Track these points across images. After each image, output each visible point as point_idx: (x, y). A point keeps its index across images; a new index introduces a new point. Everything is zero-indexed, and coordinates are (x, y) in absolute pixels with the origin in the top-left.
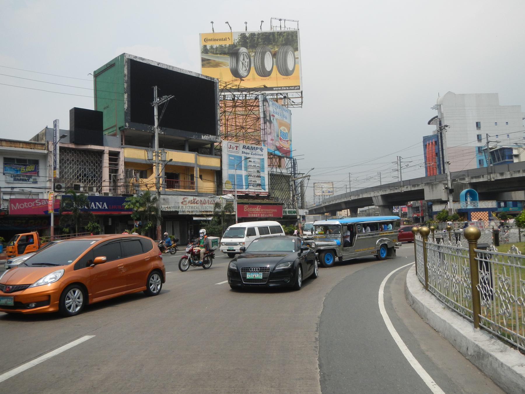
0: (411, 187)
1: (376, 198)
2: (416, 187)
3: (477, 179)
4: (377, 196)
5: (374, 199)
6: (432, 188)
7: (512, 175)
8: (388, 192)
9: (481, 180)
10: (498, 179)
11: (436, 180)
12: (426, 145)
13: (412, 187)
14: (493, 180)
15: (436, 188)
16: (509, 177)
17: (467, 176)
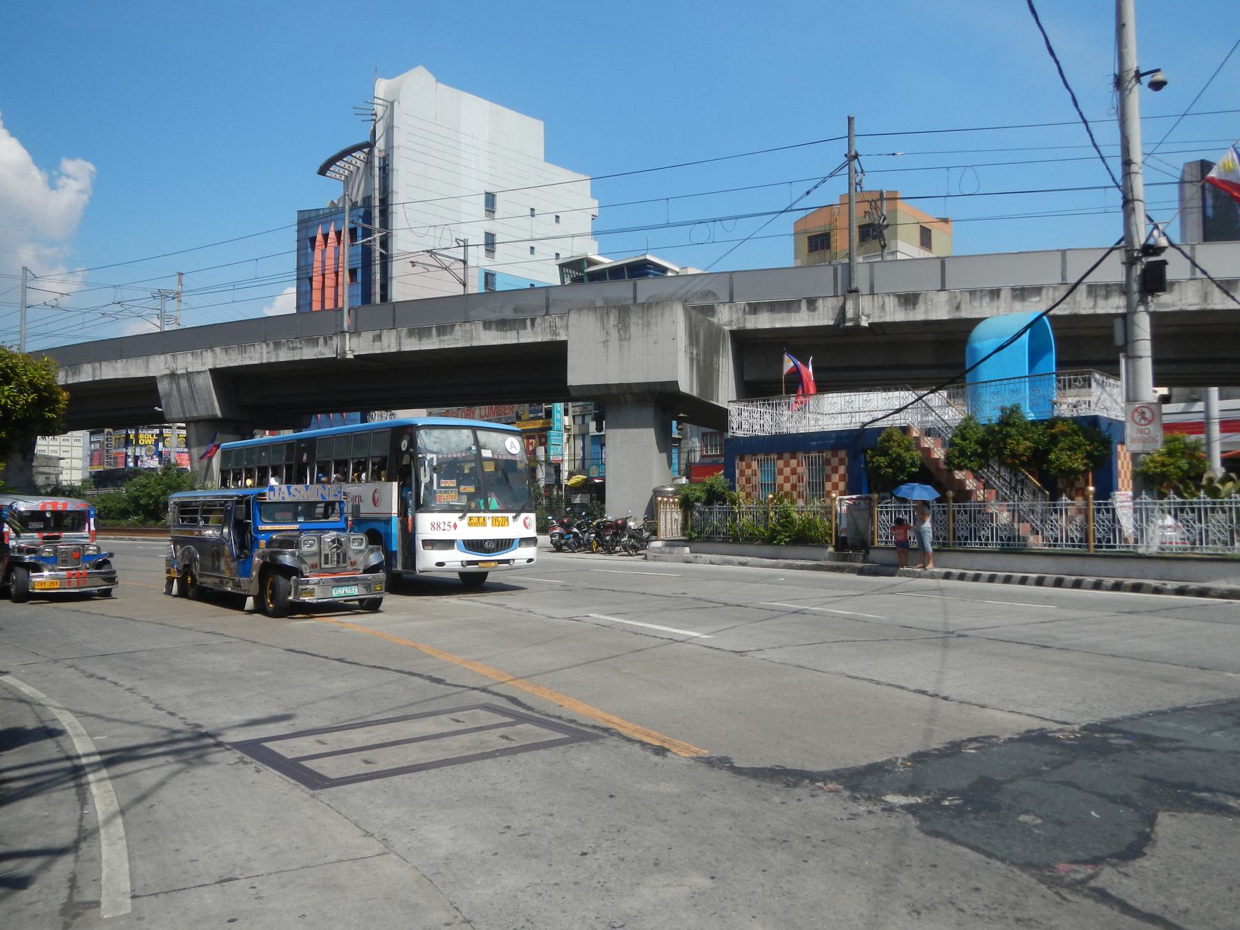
0: (399, 338)
1: (184, 383)
2: (429, 335)
3: (778, 316)
4: (189, 375)
5: (163, 387)
6: (623, 326)
7: (958, 308)
8: (258, 355)
9: (801, 319)
10: (889, 319)
11: (548, 307)
12: (313, 240)
13: (411, 333)
14: (864, 323)
15: (648, 325)
16: (945, 317)
17: (724, 296)
